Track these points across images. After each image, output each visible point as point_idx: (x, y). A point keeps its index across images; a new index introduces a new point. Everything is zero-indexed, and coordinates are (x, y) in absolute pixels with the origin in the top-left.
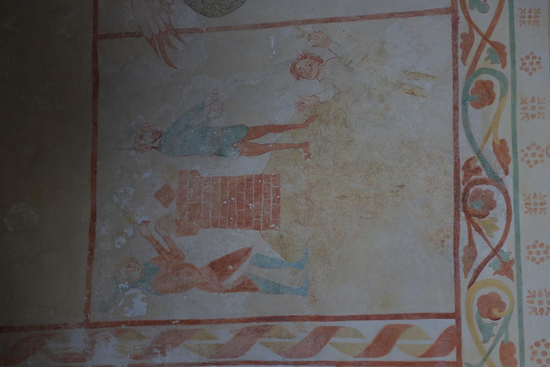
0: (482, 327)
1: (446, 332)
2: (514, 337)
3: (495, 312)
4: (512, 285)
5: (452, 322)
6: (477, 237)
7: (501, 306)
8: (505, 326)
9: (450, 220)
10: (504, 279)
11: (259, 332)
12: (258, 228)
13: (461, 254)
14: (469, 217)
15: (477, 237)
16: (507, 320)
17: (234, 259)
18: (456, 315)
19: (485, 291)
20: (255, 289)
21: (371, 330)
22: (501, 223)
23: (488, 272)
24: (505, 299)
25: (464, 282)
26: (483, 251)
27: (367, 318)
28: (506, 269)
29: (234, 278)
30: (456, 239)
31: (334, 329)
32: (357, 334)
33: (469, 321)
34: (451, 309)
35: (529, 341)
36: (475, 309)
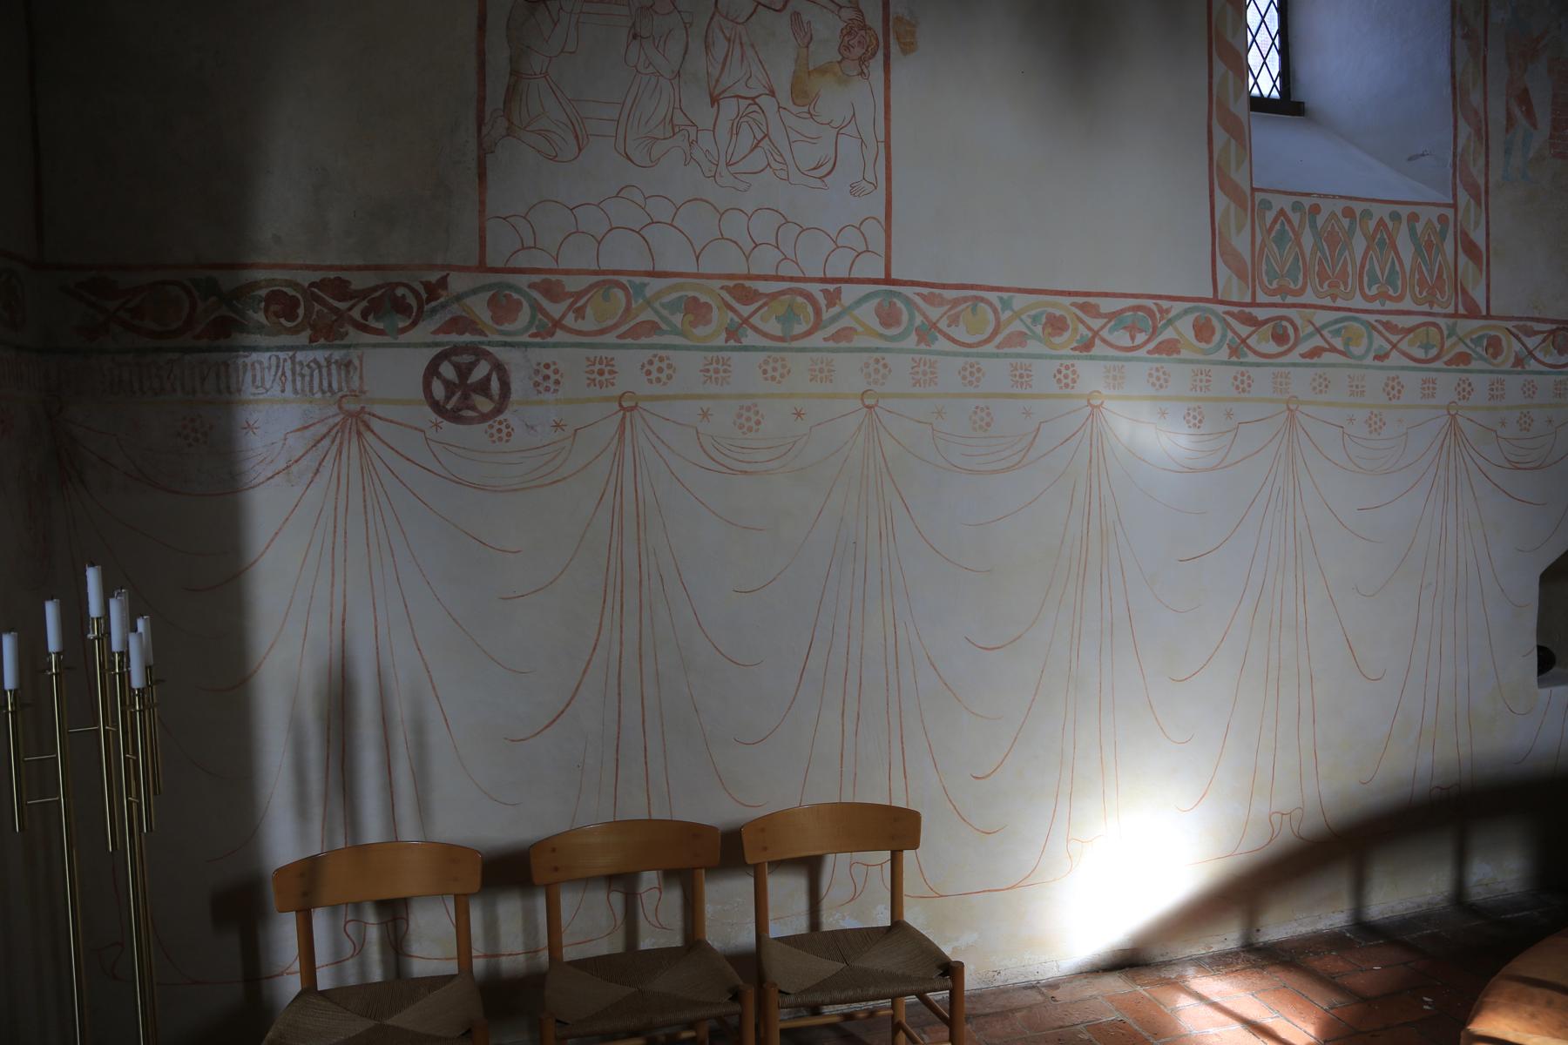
0: (1481, 338)
1: (1477, 306)
2: (1475, 365)
3: (1491, 350)
4: (1507, 367)
5: (1484, 312)
6: (1540, 338)
7: (1495, 356)
8: (1481, 358)
9: (1550, 315)
10: (1512, 359)
11: (1478, 131)
12: (1551, 137)
13: (1529, 323)
14: (1552, 332)
15: (1540, 338)
16: (1485, 360)
17: (1529, 114)
18: (1488, 316)
19: (1504, 343)
20: (1507, 131)
21: (1479, 237)
22: (1548, 360)
23: (1517, 346)
24: (1500, 359)
25: (1510, 325)
26: (1531, 342)
27: (1488, 235)
28: (1519, 361)
29: (1517, 112)
30: (1538, 320)
31: (1479, 204)
32: (1477, 224)
33: (1482, 328)
34: (1493, 313)
35: (1472, 378)
36: (1493, 333)
